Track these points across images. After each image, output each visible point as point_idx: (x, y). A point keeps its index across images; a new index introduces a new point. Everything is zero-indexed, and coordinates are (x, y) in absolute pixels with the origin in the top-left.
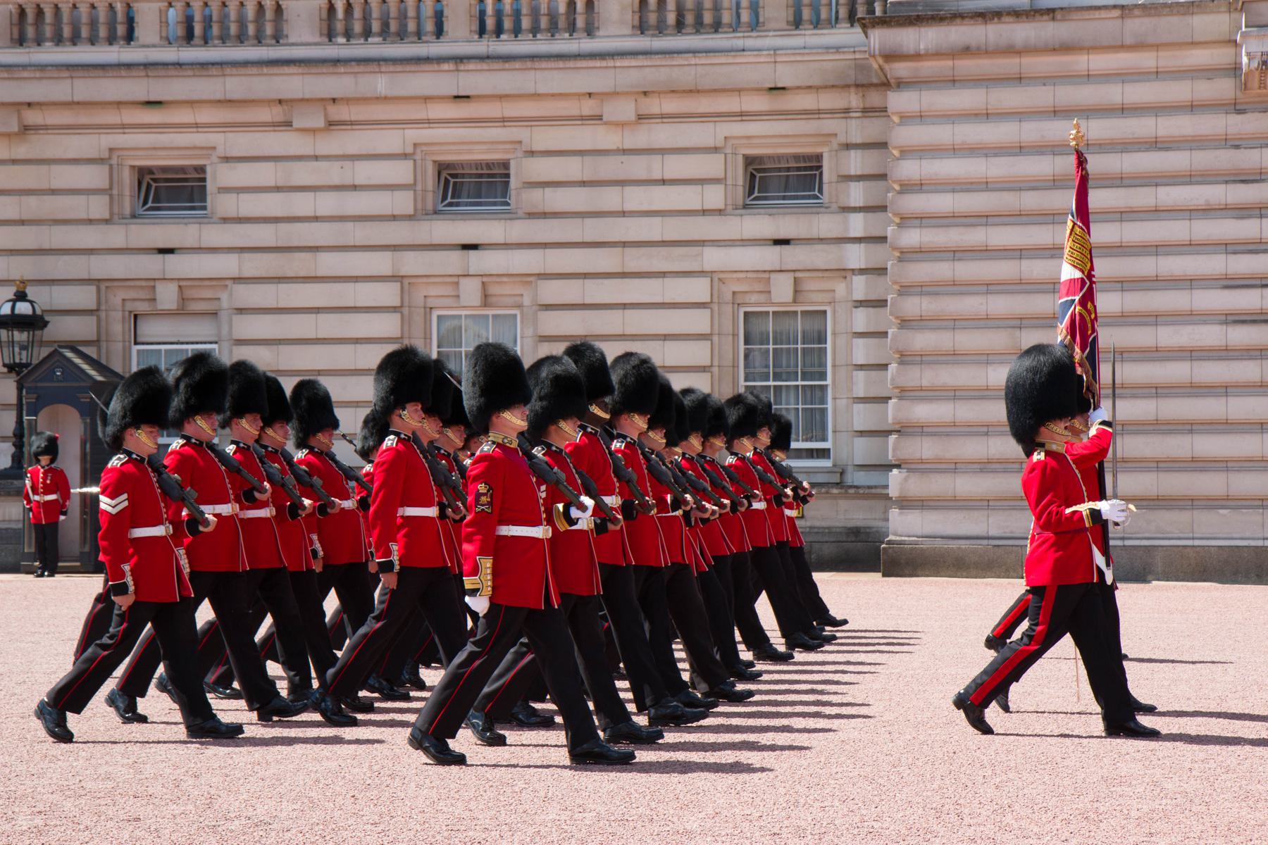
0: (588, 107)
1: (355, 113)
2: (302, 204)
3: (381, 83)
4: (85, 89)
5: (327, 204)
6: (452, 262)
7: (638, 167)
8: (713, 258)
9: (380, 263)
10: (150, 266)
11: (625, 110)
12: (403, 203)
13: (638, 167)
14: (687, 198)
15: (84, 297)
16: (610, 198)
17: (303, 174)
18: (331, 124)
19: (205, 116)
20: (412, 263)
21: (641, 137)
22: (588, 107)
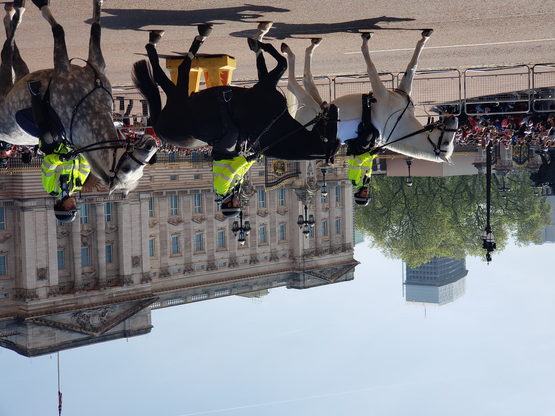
0: (166, 185)
1: (184, 184)
2: (187, 176)
3: (183, 187)
4: (204, 185)
5: (185, 176)
6: (176, 171)
7: (161, 180)
8: (155, 171)
9: (181, 170)
10: (199, 170)
11: (163, 185)
12: (155, 177)
13: (161, 180)
14: (157, 177)
15: (204, 167)
16: (163, 177)
17: (187, 179)
18: (185, 183)
19: (195, 183)
20: (179, 170)
21: (161, 183)
22: (166, 185)
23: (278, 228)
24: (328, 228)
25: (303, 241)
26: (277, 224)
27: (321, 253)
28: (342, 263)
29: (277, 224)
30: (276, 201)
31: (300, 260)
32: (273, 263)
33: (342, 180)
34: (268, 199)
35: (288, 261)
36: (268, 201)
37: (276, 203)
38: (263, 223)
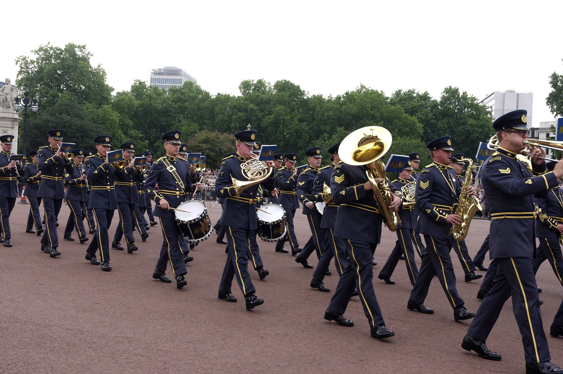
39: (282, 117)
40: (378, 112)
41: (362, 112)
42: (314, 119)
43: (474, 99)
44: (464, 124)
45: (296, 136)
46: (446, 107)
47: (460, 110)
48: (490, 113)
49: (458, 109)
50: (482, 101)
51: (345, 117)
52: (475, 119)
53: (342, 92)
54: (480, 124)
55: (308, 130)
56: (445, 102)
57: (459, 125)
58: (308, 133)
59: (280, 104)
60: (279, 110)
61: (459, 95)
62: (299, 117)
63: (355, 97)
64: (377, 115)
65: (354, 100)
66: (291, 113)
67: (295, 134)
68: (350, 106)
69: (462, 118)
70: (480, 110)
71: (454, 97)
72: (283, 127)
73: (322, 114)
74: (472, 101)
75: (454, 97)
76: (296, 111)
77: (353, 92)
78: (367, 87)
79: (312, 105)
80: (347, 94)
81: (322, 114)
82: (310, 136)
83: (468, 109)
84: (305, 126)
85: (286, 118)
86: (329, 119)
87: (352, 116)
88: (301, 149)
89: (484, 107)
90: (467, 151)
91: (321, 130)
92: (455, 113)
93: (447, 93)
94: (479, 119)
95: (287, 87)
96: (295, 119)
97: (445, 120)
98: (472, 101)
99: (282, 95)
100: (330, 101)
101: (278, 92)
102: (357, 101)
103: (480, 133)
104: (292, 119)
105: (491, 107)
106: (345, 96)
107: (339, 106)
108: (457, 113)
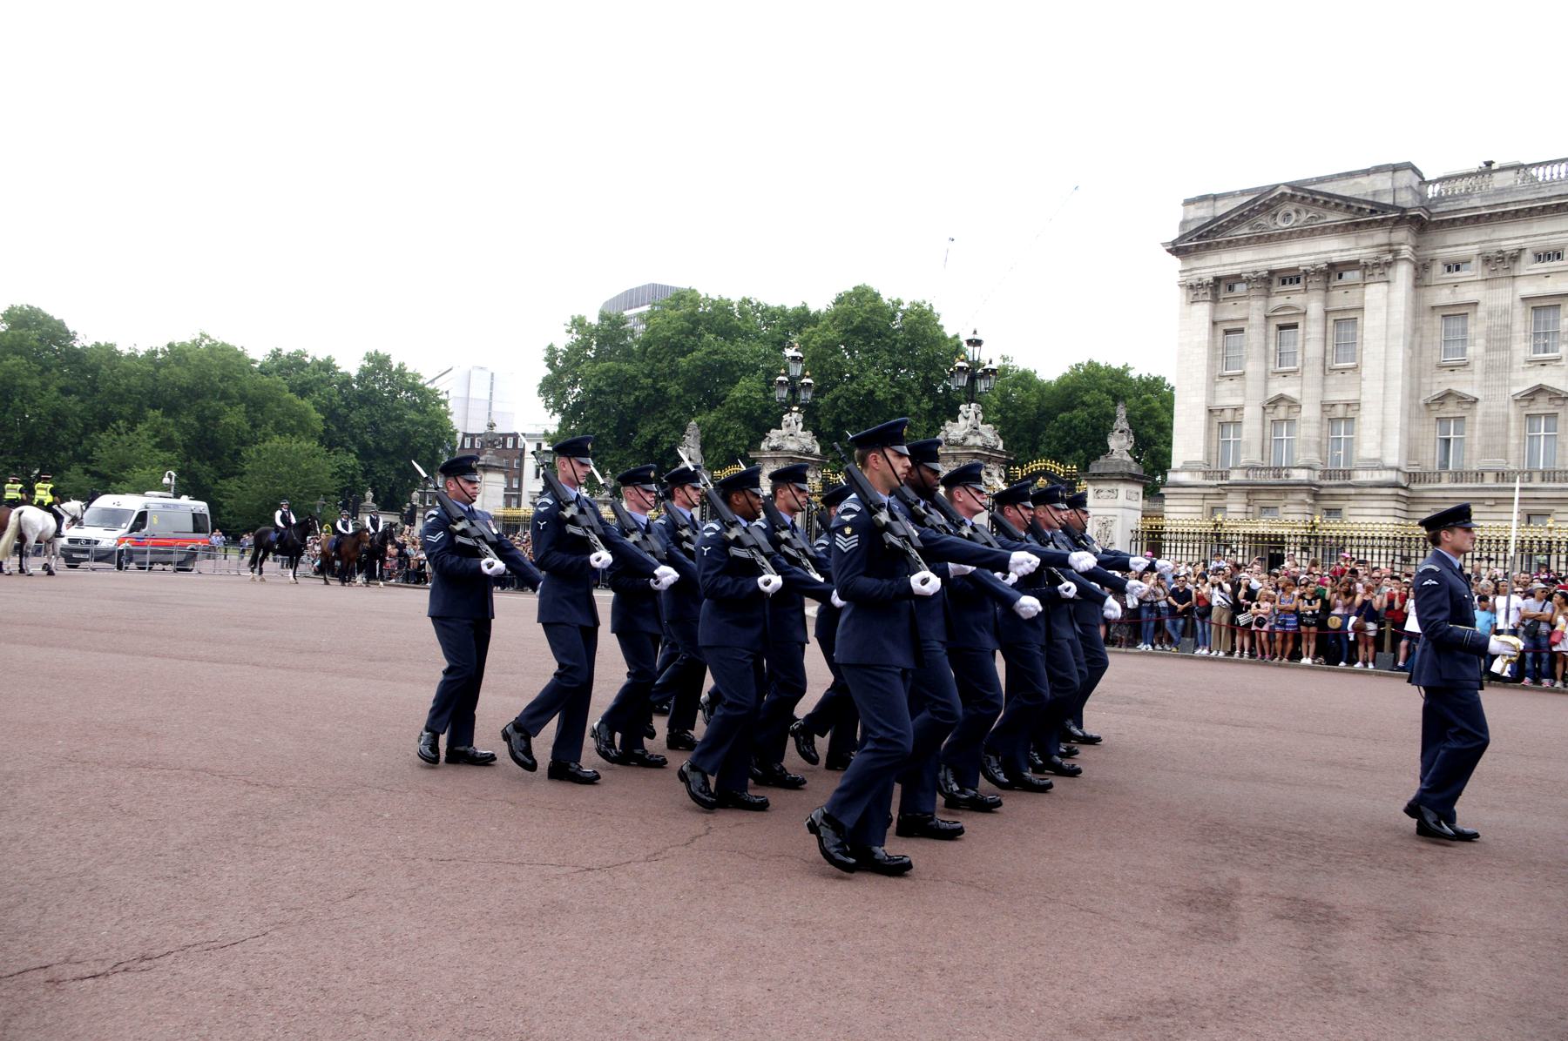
23: (1475, 350)
24: (1272, 347)
25: (1388, 306)
26: (1478, 366)
27: (1318, 272)
28: (1233, 244)
29: (1478, 366)
30: (1477, 433)
31: (1406, 251)
32: (1509, 246)
33: (1227, 482)
34: (1513, 441)
35: (1438, 251)
36: (1512, 433)
37: (1477, 426)
38: (1545, 368)
39: (19, 381)
40: (236, 385)
41: (202, 383)
42: (95, 390)
43: (417, 376)
44: (399, 418)
45: (54, 422)
46: (367, 387)
47: (393, 394)
48: (445, 402)
49: (390, 392)
50: (432, 381)
51: (166, 391)
52: (419, 411)
53: (160, 343)
54: (427, 420)
55: (81, 411)
56: (366, 378)
57: (389, 419)
58: (82, 419)
59: (16, 353)
60: (14, 366)
61: (392, 366)
62: (62, 383)
63: (188, 354)
64: (233, 391)
65: (187, 359)
66: (41, 373)
67: (50, 418)
68: (177, 370)
69: (396, 409)
70: (426, 398)
71: (381, 369)
72: (21, 401)
73: (113, 382)
74: (414, 379)
75: (381, 369)
76: (54, 370)
77: (183, 343)
78: (212, 338)
79: (91, 361)
80: (170, 345)
81: (113, 382)
82: (86, 425)
83: (406, 393)
84: (76, 404)
85: (29, 383)
86: (129, 391)
87: (181, 388)
88: (65, 449)
89: (434, 392)
90: (404, 467)
91: (111, 412)
92: (382, 399)
93: (369, 361)
94: (425, 412)
95: (34, 320)
96: (52, 388)
97: (365, 410)
98: (414, 379)
99: (22, 335)
100: (132, 357)
101: (10, 328)
102: (192, 362)
103: (427, 436)
104: (45, 386)
105: (447, 392)
106: (167, 349)
107: (153, 369)
108: (387, 399)
